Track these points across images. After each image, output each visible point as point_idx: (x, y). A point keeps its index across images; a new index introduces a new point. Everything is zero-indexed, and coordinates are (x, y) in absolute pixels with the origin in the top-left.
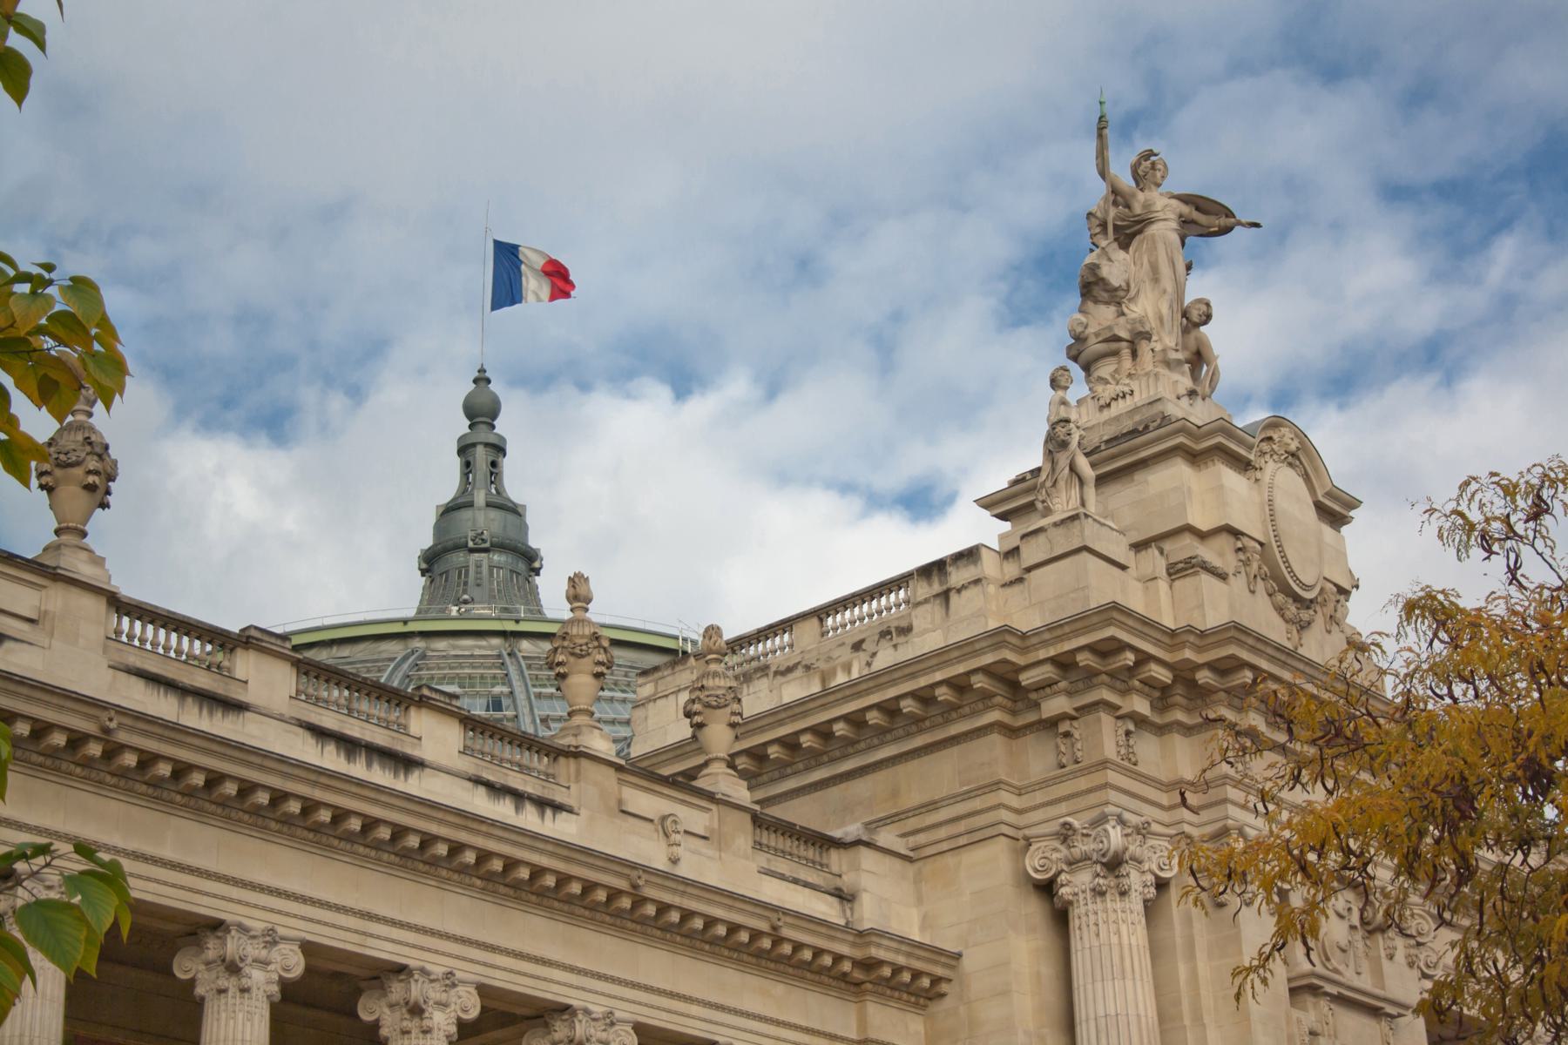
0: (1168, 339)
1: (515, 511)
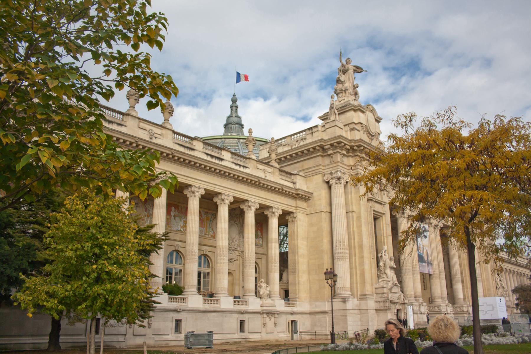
0: (351, 90)
1: (240, 118)
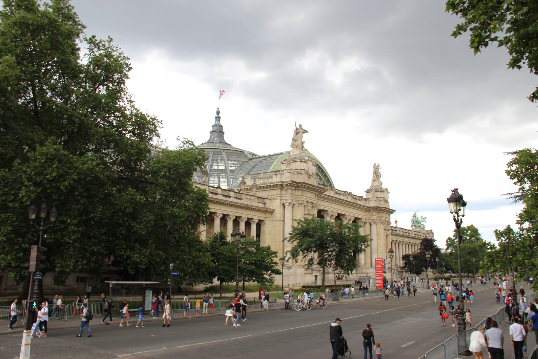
0: (300, 146)
